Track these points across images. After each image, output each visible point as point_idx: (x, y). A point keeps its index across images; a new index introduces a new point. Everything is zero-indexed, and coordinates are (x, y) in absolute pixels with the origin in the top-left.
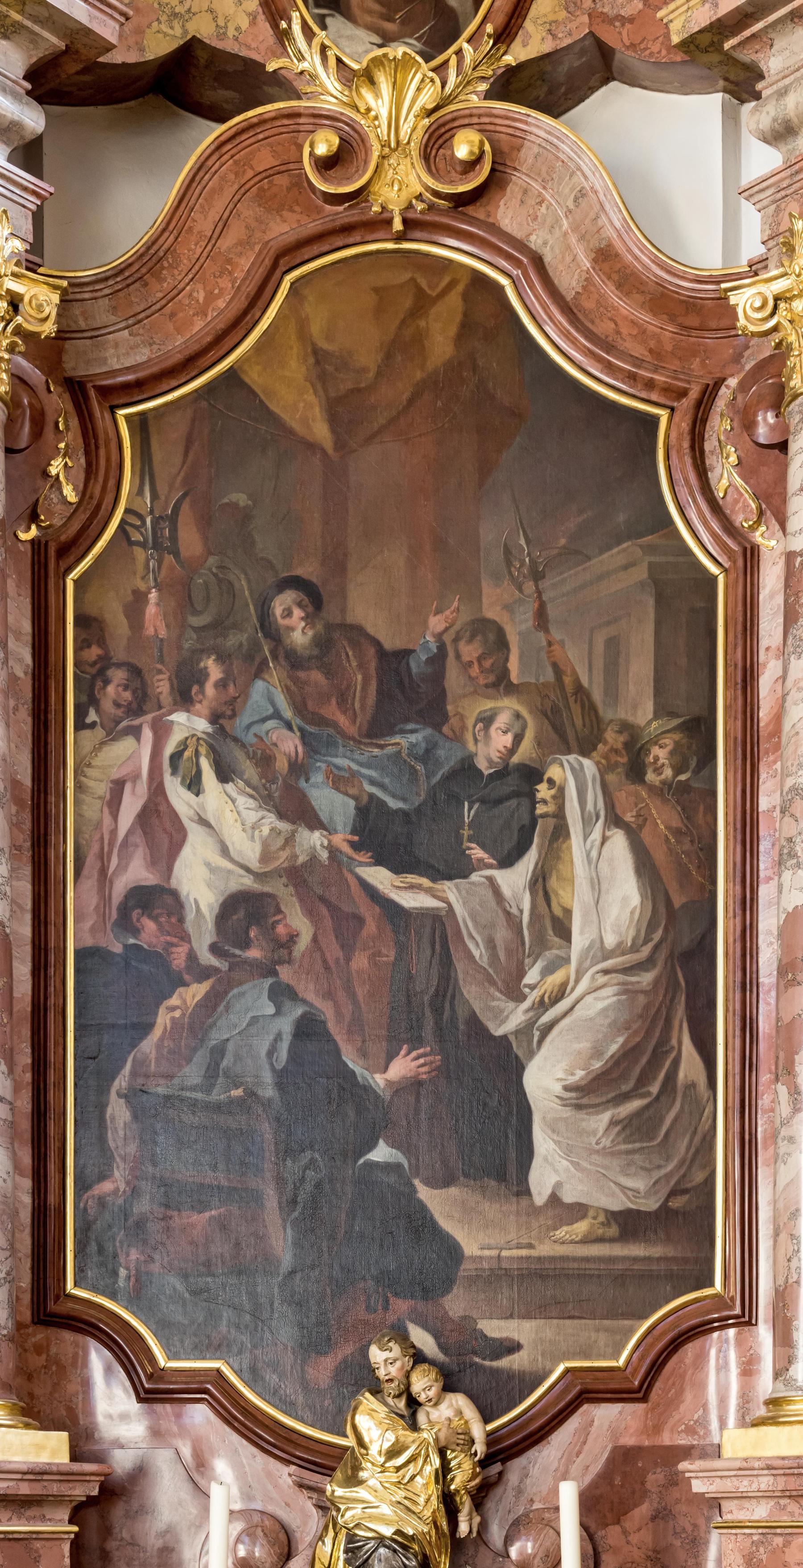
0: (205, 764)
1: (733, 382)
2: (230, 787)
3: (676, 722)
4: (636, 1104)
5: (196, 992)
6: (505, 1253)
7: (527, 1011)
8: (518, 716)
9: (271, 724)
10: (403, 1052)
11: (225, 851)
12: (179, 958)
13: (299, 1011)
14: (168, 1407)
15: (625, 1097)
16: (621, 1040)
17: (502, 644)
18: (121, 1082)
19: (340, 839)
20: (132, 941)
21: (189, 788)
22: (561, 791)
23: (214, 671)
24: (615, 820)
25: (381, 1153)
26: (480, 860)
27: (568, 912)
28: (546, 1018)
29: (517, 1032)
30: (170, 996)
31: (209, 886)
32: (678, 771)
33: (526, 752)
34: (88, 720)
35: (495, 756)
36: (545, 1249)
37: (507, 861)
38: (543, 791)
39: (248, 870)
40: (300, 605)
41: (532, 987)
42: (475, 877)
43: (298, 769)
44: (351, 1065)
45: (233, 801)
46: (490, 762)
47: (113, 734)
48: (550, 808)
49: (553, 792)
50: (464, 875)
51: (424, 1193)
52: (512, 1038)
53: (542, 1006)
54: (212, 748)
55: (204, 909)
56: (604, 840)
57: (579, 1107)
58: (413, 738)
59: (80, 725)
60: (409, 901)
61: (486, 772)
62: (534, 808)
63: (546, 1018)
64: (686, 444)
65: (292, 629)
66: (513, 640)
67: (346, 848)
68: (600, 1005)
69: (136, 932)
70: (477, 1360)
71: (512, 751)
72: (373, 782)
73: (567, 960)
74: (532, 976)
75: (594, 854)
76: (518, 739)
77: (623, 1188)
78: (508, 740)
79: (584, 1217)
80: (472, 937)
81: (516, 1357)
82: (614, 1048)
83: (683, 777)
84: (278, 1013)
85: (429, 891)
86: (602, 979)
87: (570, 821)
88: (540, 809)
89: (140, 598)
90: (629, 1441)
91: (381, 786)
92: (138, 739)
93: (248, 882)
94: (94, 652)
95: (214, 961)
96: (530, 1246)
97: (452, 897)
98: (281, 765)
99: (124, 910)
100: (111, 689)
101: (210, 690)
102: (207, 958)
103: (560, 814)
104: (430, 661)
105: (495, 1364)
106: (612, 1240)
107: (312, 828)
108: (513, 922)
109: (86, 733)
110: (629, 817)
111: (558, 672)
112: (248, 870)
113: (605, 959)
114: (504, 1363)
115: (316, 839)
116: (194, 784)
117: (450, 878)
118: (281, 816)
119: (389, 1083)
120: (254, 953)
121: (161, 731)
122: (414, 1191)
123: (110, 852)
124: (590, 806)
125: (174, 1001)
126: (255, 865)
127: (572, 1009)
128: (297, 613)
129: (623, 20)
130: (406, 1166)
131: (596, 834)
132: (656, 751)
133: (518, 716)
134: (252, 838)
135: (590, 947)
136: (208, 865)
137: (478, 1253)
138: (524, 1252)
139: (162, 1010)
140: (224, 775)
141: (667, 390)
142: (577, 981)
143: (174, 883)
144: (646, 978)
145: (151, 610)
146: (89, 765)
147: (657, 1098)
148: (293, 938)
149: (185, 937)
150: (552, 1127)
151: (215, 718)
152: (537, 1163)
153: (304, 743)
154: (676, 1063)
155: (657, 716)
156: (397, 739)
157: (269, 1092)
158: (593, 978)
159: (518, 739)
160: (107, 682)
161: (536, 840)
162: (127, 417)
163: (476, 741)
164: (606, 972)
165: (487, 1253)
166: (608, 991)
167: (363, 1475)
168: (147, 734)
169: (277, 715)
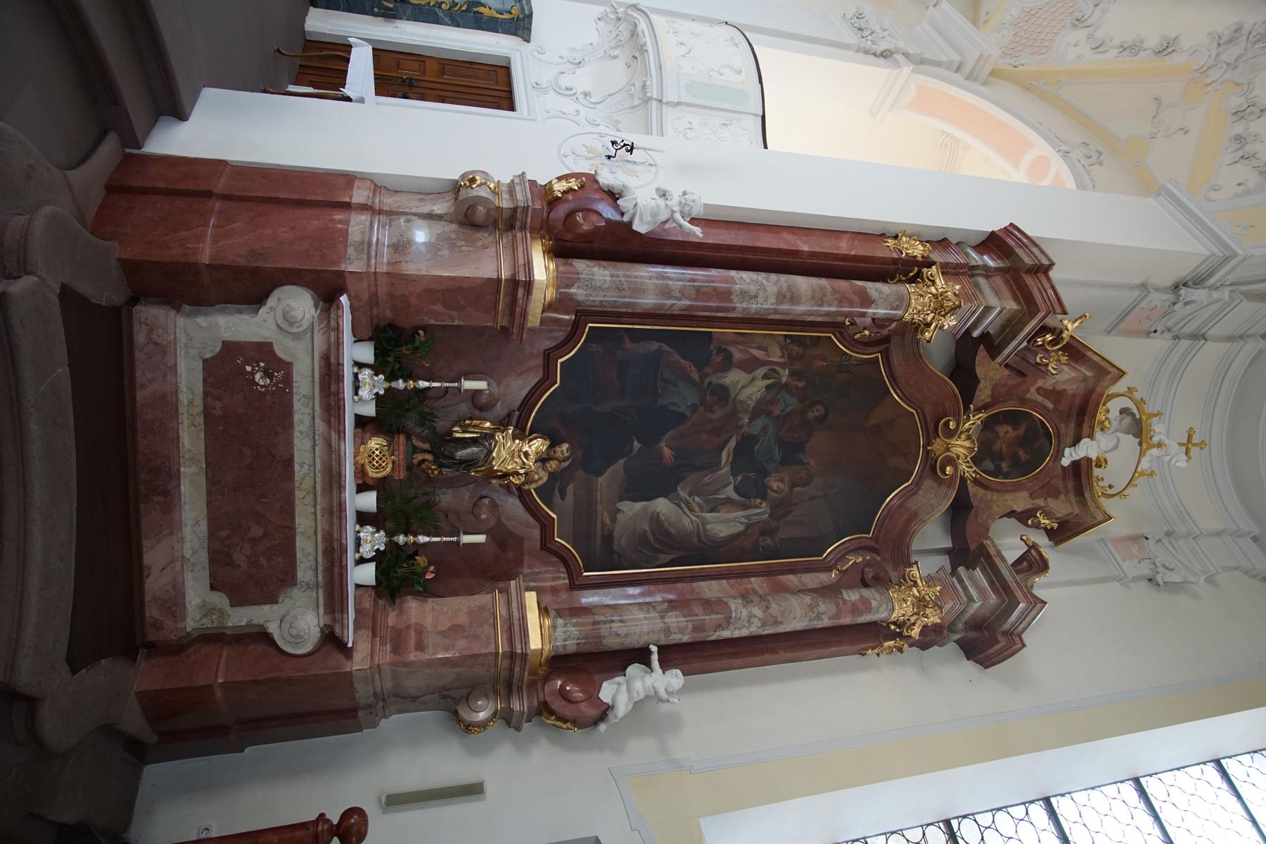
0: (772, 380)
1: (879, 558)
2: (764, 390)
3: (778, 545)
4: (652, 540)
5: (696, 376)
6: (599, 493)
7: (686, 499)
8: (782, 491)
9: (784, 404)
10: (673, 453)
11: (743, 387)
12: (708, 370)
13: (688, 414)
14: (542, 362)
15: (654, 534)
16: (674, 532)
17: (804, 486)
18: (666, 348)
19: (745, 428)
20: (714, 353)
21: (764, 375)
22: (757, 507)
23: (801, 385)
24: (748, 526)
25: (636, 445)
26: (737, 479)
27: (717, 512)
28: (683, 505)
29: (678, 494)
30: (695, 367)
31: (733, 381)
32: (763, 547)
33: (771, 494)
34: (787, 340)
35: (771, 483)
36: (600, 507)
37: (736, 489)
38: (758, 501)
39: (736, 397)
40: (820, 415)
41: (693, 500)
42: (731, 477)
43: (769, 414)
44: (668, 434)
45: (760, 391)
46: (768, 482)
47: (782, 348)
48: (753, 504)
49: (758, 504)
50: (732, 474)
51: (622, 461)
52: (676, 493)
53: (687, 503)
54: (777, 383)
55: (724, 380)
56: (742, 523)
57: (651, 518)
58: (777, 454)
59: (785, 336)
60: (724, 454)
61: (765, 481)
62: (753, 498)
63: (683, 505)
64: (862, 545)
65: (813, 412)
66: (806, 488)
67: (743, 431)
68: (686, 524)
69: (717, 354)
70: (558, 483)
71: (772, 490)
72: (763, 441)
73: (702, 512)
74: (697, 499)
75: (737, 520)
76: (775, 491)
77: (621, 537)
78: (775, 488)
79: (612, 522)
80: (711, 477)
81: (559, 498)
82: (672, 530)
83: (760, 549)
84: (687, 406)
85: (727, 461)
86: (695, 525)
87: (748, 511)
88: (752, 500)
89: (824, 359)
90: (526, 543)
91: (762, 444)
92: (781, 357)
93: (733, 396)
94: (808, 342)
95: (706, 383)
96: (601, 502)
97: (725, 469)
98: (770, 408)
99: (725, 350)
100: (797, 348)
101: (795, 383)
102: (707, 381)
103: (751, 507)
104: (801, 460)
105: (556, 491)
106: (603, 532)
107: (749, 419)
108: (717, 492)
109: (783, 338)
110: (749, 531)
111: (795, 504)
112: (737, 395)
113: (702, 525)
114: (557, 495)
115: (746, 420)
116: (765, 377)
117: (731, 469)
118: (754, 408)
119: (662, 447)
120: (708, 397)
121: (782, 365)
122: (623, 458)
123: (743, 346)
124: (753, 517)
125: (693, 368)
126: (738, 398)
127: (686, 514)
128: (818, 414)
129: (976, 517)
130: (633, 454)
131: (744, 520)
132: (770, 539)
133: (782, 491)
134: (747, 397)
135: (707, 520)
136: (738, 382)
137: (599, 482)
138: (599, 500)
139: (690, 363)
140: (768, 387)
141: (877, 537)
142: (695, 516)
143: (733, 368)
144: (695, 540)
145: (821, 363)
146: (773, 339)
147: (654, 547)
148: (713, 412)
149: (715, 372)
150: (644, 508)
151: (785, 384)
152: (632, 503)
153: (777, 416)
154: (666, 553)
155: (780, 539)
156: (777, 449)
157: (660, 402)
158: (696, 521)
159: (775, 491)
160: (799, 346)
161: (743, 499)
162: (878, 357)
163: (775, 477)
164: (698, 525)
165: (599, 486)
166: (692, 528)
167: (517, 441)
168: (782, 360)
169: (786, 406)
